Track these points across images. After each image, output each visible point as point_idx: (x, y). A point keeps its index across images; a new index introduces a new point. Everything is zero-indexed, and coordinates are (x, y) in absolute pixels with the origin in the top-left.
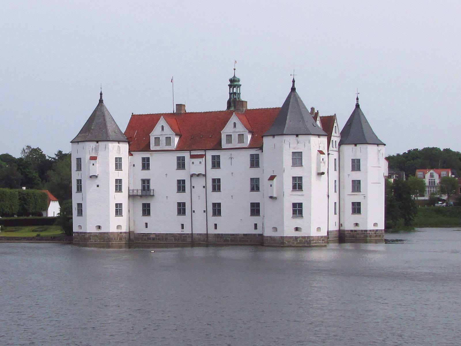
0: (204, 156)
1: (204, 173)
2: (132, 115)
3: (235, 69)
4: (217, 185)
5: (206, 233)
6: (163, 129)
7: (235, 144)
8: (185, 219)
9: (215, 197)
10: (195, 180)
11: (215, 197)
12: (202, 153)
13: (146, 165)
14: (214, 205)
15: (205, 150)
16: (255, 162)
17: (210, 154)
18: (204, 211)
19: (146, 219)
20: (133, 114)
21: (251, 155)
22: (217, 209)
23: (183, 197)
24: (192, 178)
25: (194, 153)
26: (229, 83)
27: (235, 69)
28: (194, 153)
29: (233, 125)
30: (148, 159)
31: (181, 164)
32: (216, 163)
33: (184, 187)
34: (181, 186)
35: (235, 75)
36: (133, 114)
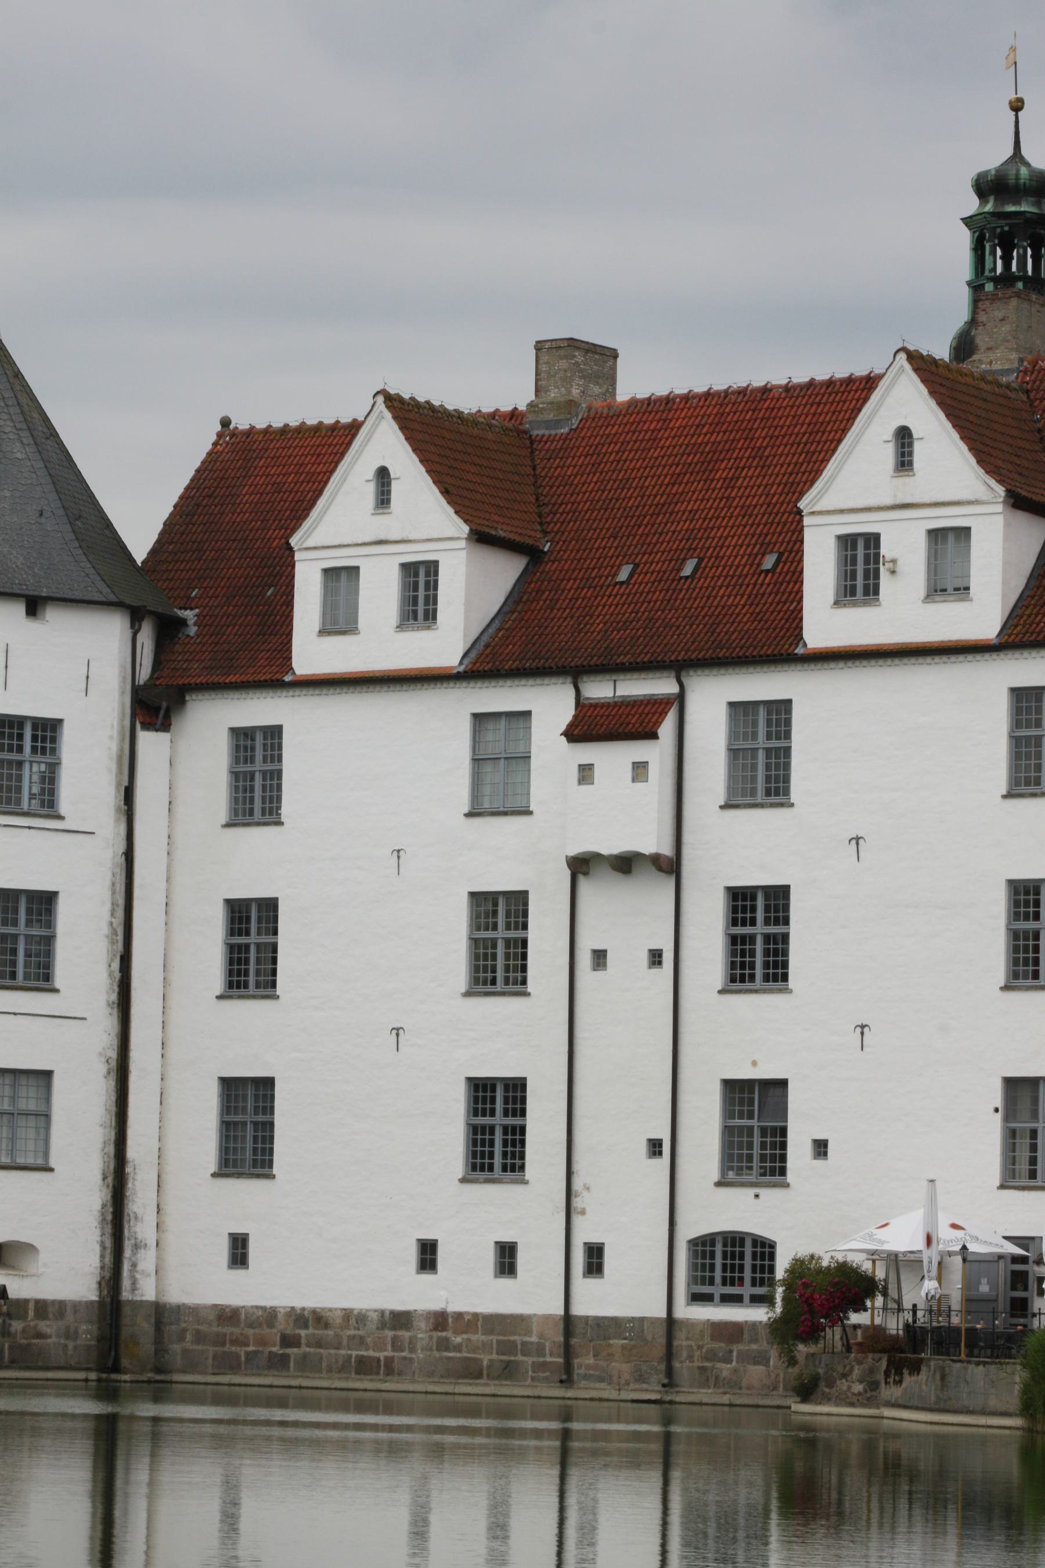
0: (663, 714)
1: (667, 850)
2: (220, 435)
3: (1017, 106)
5: (663, 1314)
6: (383, 499)
12: (663, 686)
18: (655, 1147)
20: (225, 423)
24: (583, 884)
25: (599, 690)
26: (971, 204)
27: (1017, 106)
28: (599, 690)
29: (888, 454)
30: (274, 733)
35: (1025, 152)
36: (225, 423)
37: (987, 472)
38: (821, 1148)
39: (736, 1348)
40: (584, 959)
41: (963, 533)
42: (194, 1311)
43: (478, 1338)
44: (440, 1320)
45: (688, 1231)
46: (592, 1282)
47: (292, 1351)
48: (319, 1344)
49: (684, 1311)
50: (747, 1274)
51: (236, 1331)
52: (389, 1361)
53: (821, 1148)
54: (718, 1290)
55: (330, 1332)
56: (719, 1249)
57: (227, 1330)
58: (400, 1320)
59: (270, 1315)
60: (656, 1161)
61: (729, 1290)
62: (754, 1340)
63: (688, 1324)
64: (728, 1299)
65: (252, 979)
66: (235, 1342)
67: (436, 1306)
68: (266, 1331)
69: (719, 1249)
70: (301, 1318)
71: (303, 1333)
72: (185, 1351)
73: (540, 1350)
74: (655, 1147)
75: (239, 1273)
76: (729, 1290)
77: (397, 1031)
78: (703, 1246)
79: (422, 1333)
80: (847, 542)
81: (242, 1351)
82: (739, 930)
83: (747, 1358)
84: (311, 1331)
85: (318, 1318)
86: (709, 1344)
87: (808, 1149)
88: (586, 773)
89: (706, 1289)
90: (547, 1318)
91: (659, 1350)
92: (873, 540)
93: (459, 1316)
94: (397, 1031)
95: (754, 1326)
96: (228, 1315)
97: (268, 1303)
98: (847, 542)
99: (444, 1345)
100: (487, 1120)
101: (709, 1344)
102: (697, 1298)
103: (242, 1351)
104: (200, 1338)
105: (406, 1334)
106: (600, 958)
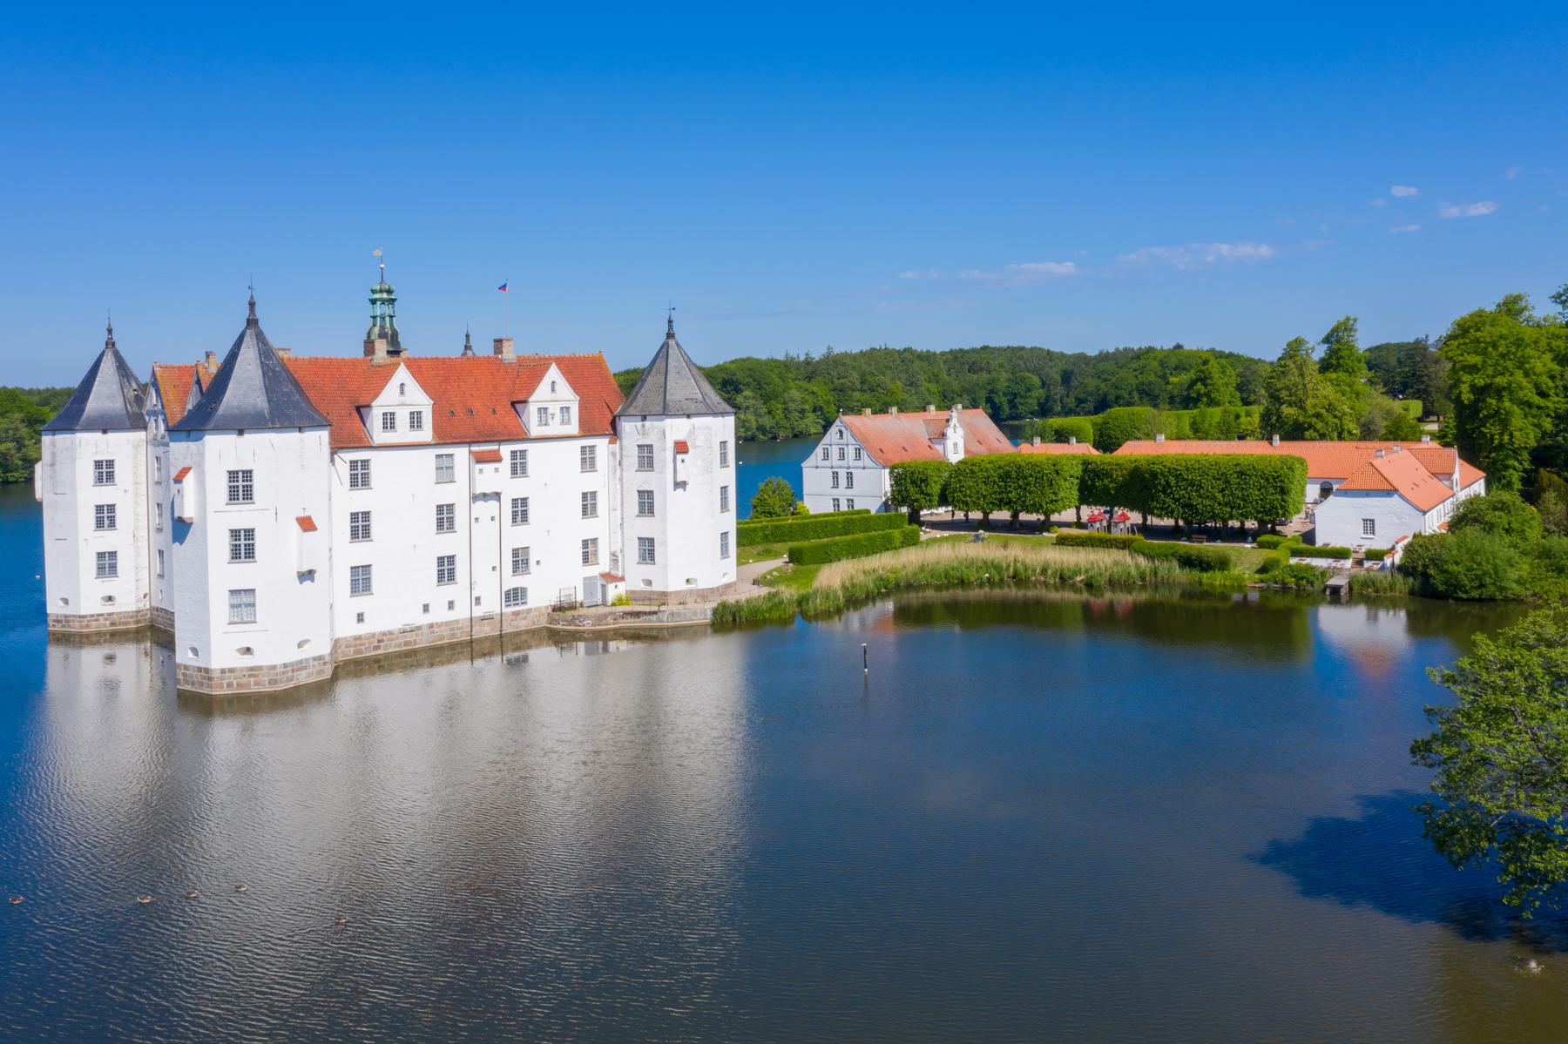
4: (520, 510)
5: (499, 612)
7: (555, 428)
8: (457, 590)
9: (517, 536)
10: (480, 504)
11: (517, 536)
12: (493, 447)
13: (360, 477)
14: (516, 553)
15: (500, 442)
16: (588, 460)
17: (506, 450)
18: (494, 568)
19: (362, 603)
21: (582, 447)
22: (520, 560)
23: (448, 544)
28: (475, 448)
31: (445, 472)
32: (519, 467)
33: (451, 520)
34: (445, 518)
37: (576, 393)
38: (538, 562)
39: (518, 617)
40: (473, 520)
41: (568, 408)
42: (345, 639)
43: (443, 628)
44: (431, 626)
45: (504, 589)
46: (478, 607)
47: (381, 644)
48: (391, 640)
49: (505, 610)
50: (512, 598)
51: (361, 642)
52: (415, 641)
53: (538, 562)
54: (512, 603)
55: (394, 636)
56: (512, 592)
57: (358, 642)
58: (419, 628)
59: (373, 635)
60: (494, 572)
61: (515, 602)
62: (523, 613)
63: (506, 614)
64: (515, 604)
65: (360, 535)
66: (361, 645)
67: (430, 622)
68: (372, 640)
69: (512, 592)
70: (384, 634)
71: (385, 638)
72: (342, 652)
73: (462, 628)
74: (494, 568)
75: (361, 624)
76: (515, 602)
77: (415, 546)
78: (508, 593)
79: (425, 630)
80: (540, 409)
81: (363, 648)
82: (525, 508)
83: (521, 619)
84: (388, 637)
85: (390, 633)
86: (511, 617)
87: (535, 563)
88: (481, 471)
89: (508, 603)
90: (466, 619)
91: (499, 622)
92: (546, 409)
93: (437, 623)
94: (415, 546)
95: (523, 610)
96: (358, 638)
97: (373, 632)
98: (540, 409)
99: (432, 632)
100: (442, 568)
101: (511, 617)
102: (507, 606)
103: (363, 648)
104: (347, 646)
105: (420, 632)
106: (477, 519)
